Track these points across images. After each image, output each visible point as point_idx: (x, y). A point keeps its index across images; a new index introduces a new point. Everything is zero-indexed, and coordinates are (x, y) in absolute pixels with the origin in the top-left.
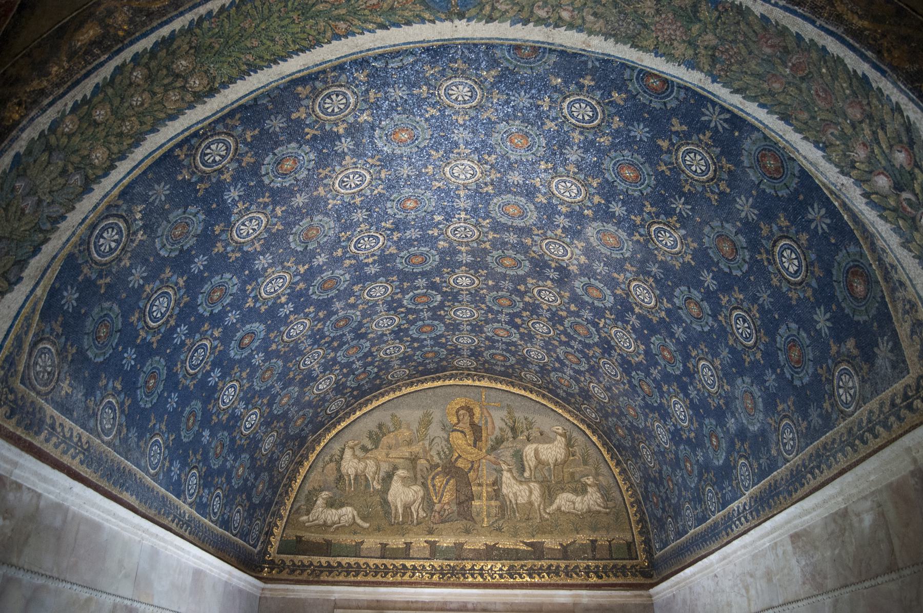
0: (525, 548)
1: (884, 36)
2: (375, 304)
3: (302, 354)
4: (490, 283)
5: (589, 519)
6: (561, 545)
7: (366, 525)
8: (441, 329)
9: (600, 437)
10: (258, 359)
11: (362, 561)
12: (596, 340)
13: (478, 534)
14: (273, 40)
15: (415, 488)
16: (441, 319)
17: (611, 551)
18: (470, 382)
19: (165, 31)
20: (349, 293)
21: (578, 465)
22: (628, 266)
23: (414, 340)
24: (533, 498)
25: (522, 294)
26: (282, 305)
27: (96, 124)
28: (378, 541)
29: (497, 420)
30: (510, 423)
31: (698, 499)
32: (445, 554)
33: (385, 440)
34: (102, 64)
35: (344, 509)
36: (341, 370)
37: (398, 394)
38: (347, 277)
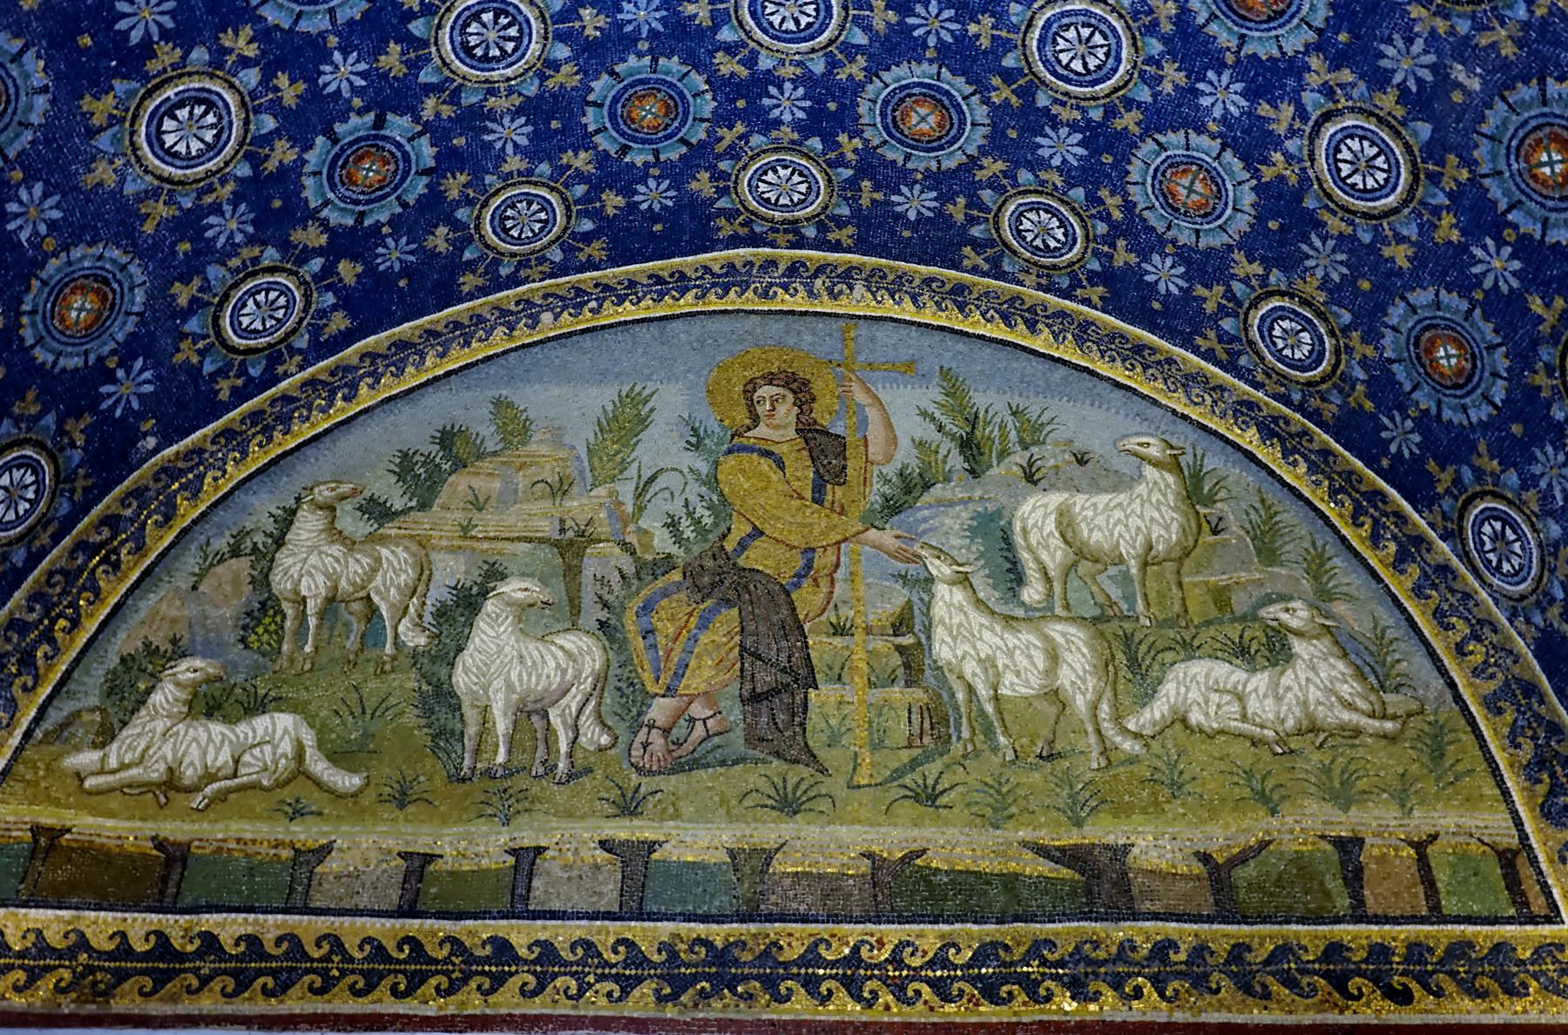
0: (1044, 867)
6: (1205, 858)
7: (348, 781)
9: (1321, 462)
11: (308, 927)
13: (835, 814)
15: (570, 641)
17: (1429, 883)
18: (799, 302)
21: (1245, 565)
24: (1065, 677)
28: (394, 844)
29: (898, 420)
30: (957, 428)
32: (687, 891)
33: (460, 483)
35: (262, 723)
37: (523, 336)
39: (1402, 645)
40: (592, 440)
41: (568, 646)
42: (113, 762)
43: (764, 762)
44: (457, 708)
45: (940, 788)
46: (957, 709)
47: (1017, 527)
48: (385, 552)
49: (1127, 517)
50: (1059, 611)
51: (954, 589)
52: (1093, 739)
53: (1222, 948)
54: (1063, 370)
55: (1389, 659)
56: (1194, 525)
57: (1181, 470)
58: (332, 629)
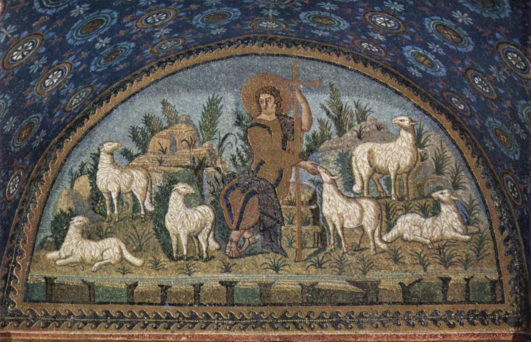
5: (441, 249)
7: (138, 262)
39: (478, 207)
40: (201, 121)
41: (201, 210)
42: (63, 256)
43: (268, 253)
44: (168, 234)
45: (323, 261)
46: (329, 233)
47: (353, 158)
48: (134, 173)
49: (393, 154)
50: (365, 195)
51: (330, 185)
52: (372, 244)
53: (402, 313)
54: (376, 85)
55: (473, 213)
56: (415, 157)
57: (415, 132)
58: (122, 204)
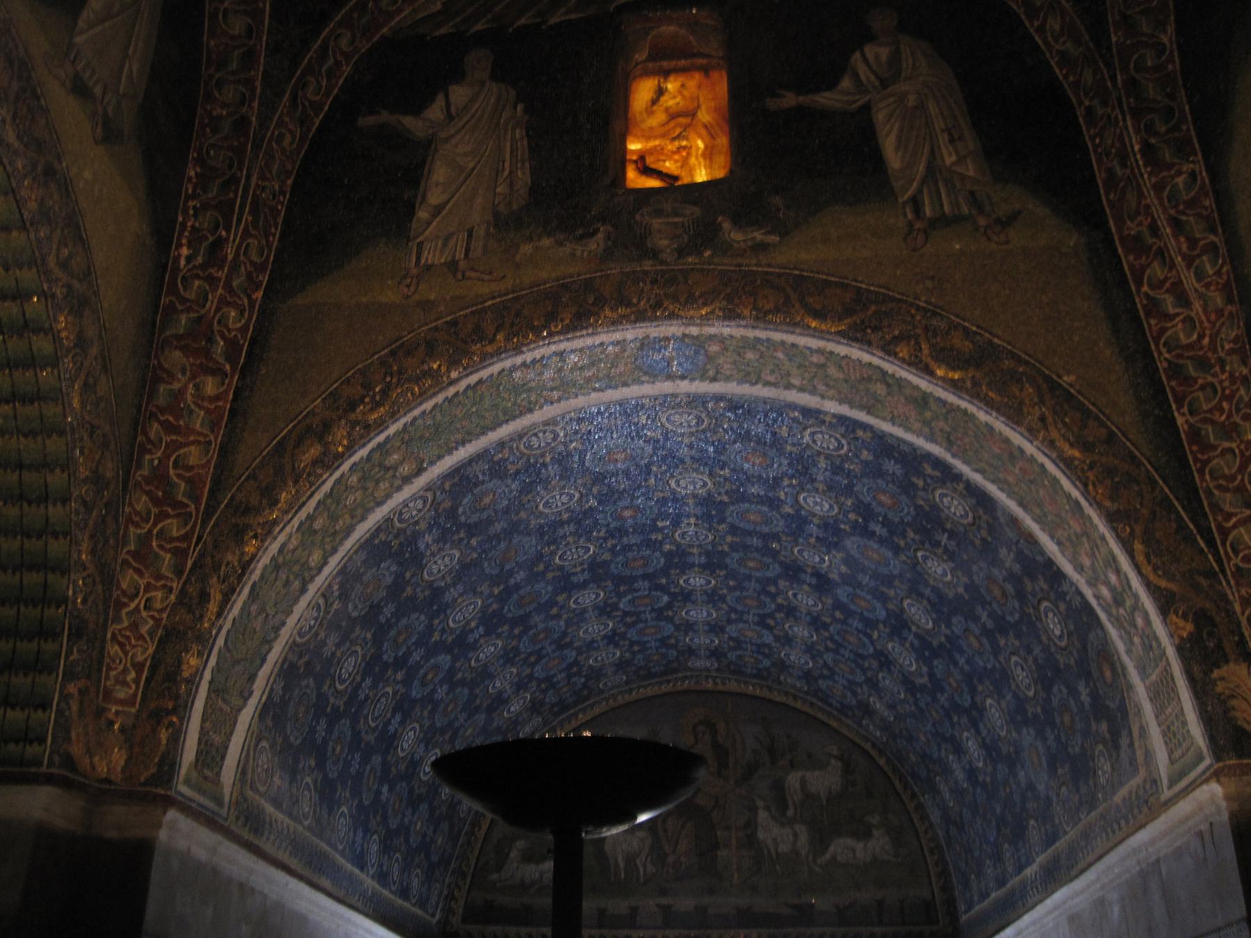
1: (1091, 467)
2: (584, 611)
3: (491, 677)
4: (731, 583)
8: (669, 629)
10: (441, 692)
12: (871, 650)
14: (483, 417)
16: (670, 620)
19: (381, 438)
20: (552, 603)
22: (897, 582)
23: (632, 643)
25: (773, 597)
26: (472, 631)
27: (316, 532)
31: (998, 857)
34: (324, 482)
36: (539, 685)
38: (550, 588)
